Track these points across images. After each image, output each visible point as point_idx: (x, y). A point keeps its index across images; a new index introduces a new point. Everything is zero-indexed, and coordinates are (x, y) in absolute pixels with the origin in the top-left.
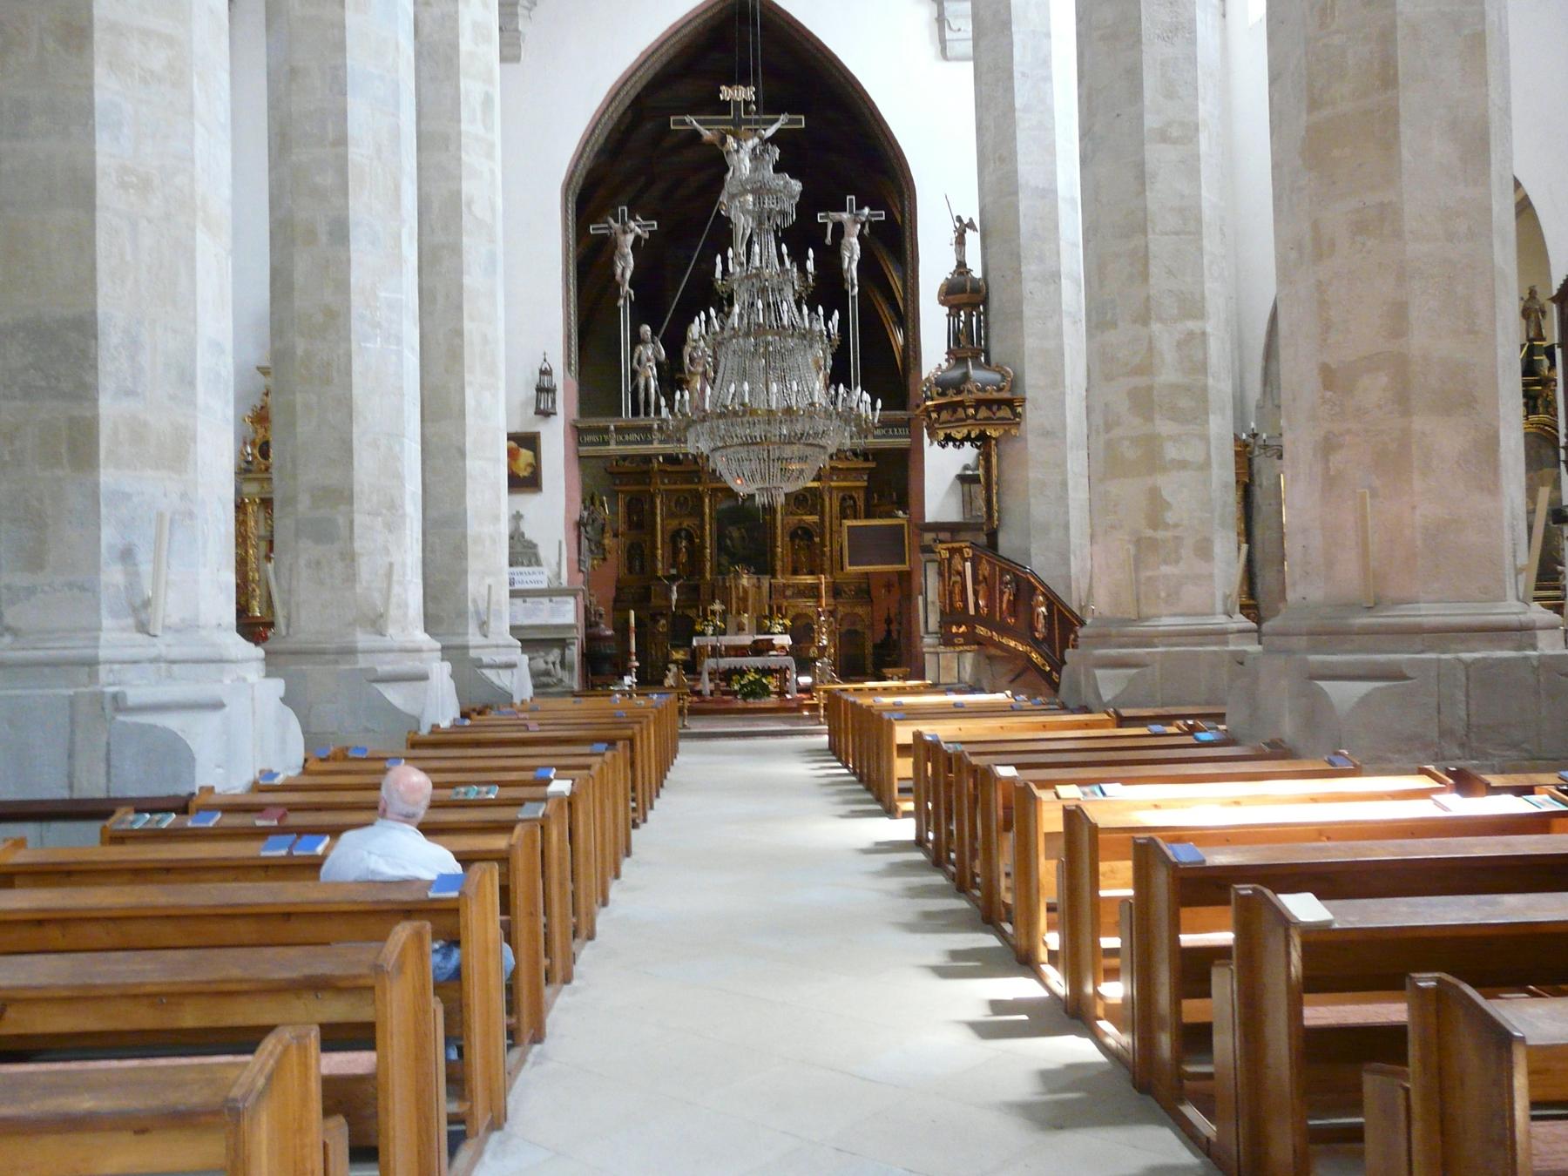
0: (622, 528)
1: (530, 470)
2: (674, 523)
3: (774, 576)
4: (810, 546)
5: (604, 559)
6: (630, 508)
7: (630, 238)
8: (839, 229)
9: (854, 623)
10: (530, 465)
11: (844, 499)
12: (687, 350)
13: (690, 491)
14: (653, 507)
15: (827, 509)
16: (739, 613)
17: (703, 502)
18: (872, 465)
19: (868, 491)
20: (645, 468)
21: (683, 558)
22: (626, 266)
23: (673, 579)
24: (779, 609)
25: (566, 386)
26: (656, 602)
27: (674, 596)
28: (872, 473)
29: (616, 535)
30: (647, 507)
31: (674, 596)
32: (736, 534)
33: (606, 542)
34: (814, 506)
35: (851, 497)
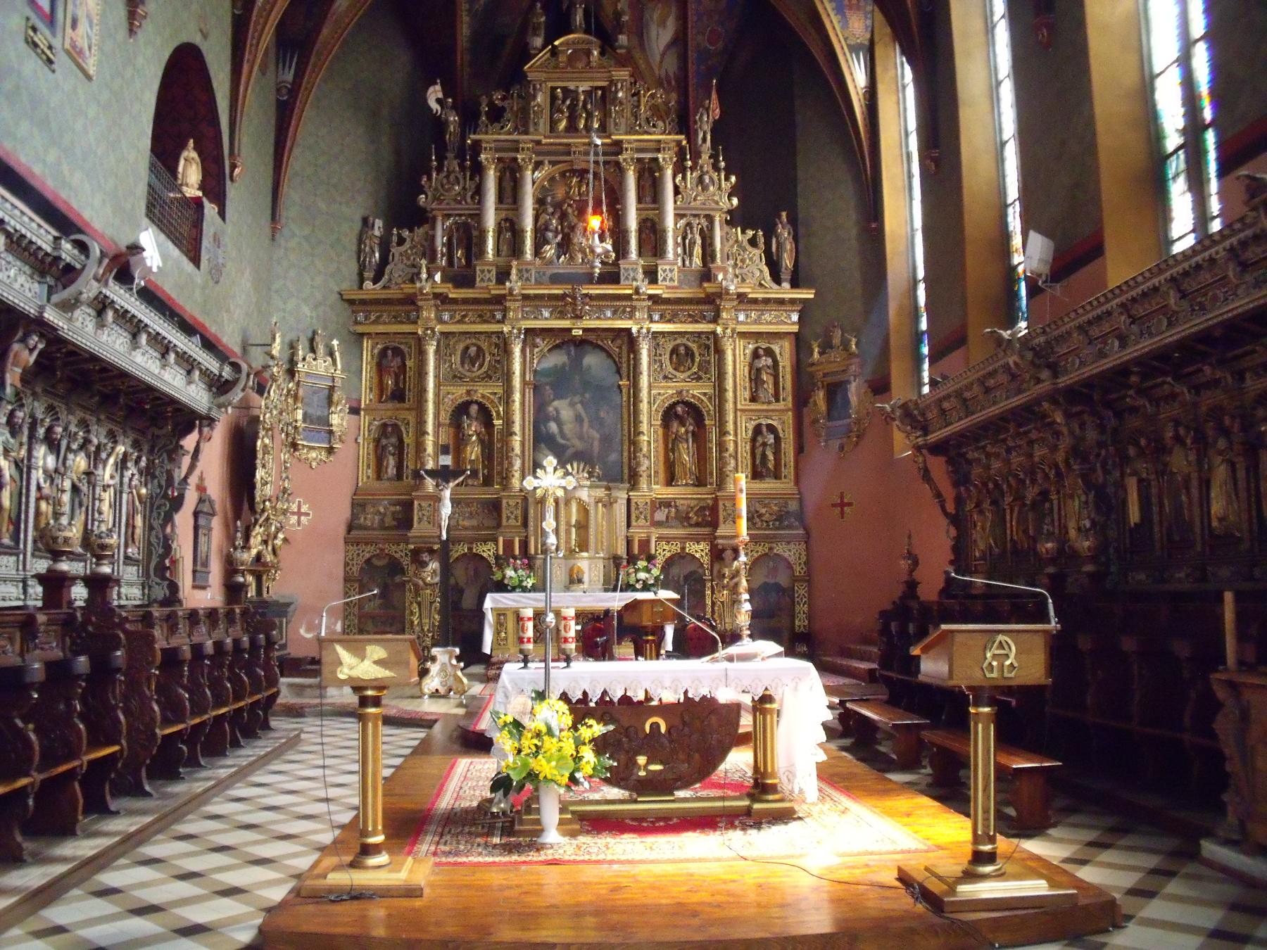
0: (366, 398)
2: (458, 393)
3: (634, 485)
4: (699, 436)
5: (330, 450)
6: (381, 368)
9: (775, 569)
11: (756, 355)
13: (489, 334)
14: (422, 353)
15: (730, 369)
16: (571, 553)
17: (507, 352)
18: (808, 294)
19: (800, 341)
20: (408, 289)
21: (473, 452)
23: (443, 475)
24: (645, 544)
26: (419, 528)
27: (446, 510)
28: (805, 308)
29: (355, 411)
30: (409, 363)
31: (446, 510)
32: (566, 414)
33: (335, 420)
34: (704, 367)
35: (769, 352)
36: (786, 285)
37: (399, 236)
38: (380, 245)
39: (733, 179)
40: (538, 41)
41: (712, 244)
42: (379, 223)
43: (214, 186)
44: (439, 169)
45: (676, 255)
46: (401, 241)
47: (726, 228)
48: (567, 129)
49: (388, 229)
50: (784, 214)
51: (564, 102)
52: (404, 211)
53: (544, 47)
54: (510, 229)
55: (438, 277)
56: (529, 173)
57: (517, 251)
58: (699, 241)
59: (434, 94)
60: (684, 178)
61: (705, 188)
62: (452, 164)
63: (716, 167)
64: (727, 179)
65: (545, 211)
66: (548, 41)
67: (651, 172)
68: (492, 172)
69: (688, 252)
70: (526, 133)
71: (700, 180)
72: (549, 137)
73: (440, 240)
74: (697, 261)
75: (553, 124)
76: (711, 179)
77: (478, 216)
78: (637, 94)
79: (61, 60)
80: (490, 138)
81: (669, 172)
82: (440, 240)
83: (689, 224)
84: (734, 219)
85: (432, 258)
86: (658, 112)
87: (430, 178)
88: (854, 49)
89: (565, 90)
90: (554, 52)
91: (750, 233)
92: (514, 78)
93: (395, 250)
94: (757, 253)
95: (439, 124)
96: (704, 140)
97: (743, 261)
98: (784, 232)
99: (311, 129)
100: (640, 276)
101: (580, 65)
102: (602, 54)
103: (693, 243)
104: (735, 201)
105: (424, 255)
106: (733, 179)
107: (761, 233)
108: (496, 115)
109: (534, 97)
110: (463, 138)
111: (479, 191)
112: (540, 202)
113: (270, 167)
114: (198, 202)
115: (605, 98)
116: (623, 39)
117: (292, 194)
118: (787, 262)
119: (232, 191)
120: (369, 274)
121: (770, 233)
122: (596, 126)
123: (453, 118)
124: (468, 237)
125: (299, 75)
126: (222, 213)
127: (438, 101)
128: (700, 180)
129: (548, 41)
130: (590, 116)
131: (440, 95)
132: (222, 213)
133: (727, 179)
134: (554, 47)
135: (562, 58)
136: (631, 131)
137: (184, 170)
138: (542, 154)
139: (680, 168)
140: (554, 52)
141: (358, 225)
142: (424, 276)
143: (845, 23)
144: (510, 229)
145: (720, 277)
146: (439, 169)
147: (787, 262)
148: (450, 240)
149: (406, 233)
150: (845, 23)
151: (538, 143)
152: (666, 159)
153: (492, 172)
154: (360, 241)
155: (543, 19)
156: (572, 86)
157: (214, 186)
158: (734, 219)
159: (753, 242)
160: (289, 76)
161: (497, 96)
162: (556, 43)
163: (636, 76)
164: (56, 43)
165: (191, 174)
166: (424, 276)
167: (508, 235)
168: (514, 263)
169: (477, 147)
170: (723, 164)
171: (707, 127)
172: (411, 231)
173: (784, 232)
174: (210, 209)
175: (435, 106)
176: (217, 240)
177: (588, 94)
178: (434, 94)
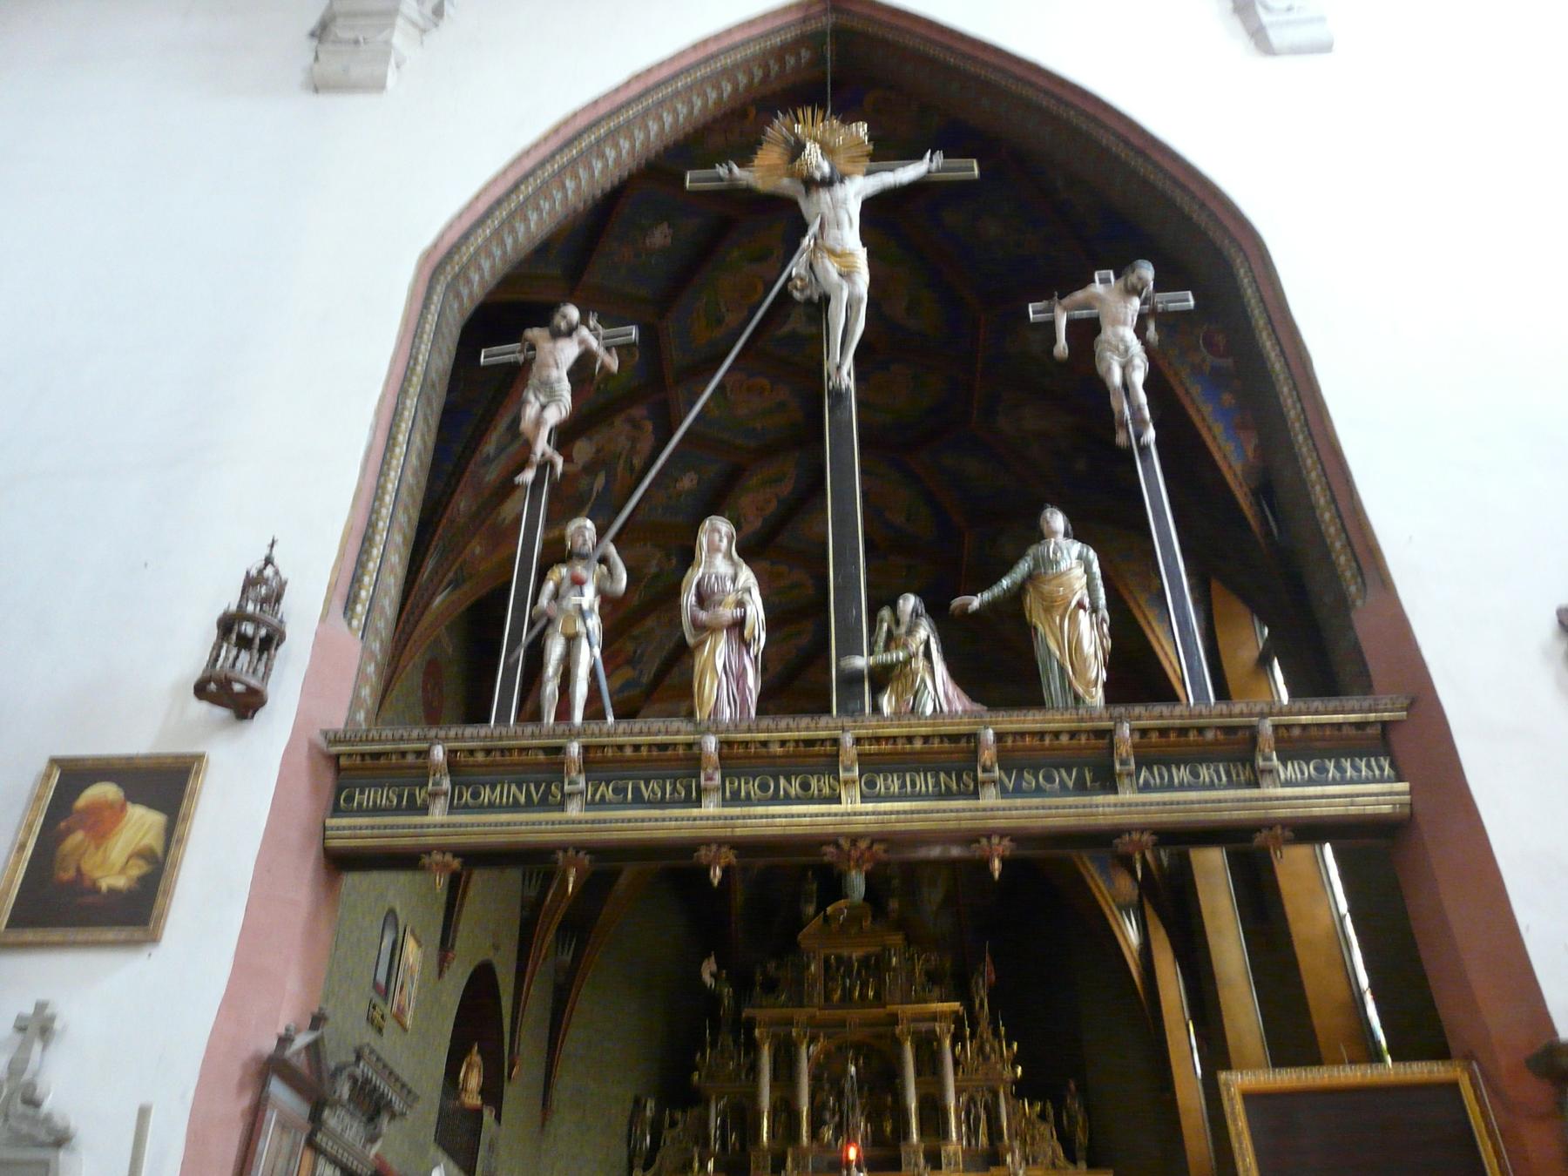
1: (138, 869)
7: (568, 352)
8: (1087, 331)
10: (145, 855)
12: (695, 575)
22: (547, 409)
25: (321, 642)
36: (1083, 1165)
37: (671, 1116)
38: (652, 1127)
39: (1015, 1046)
40: (811, 910)
41: (998, 1118)
42: (650, 1105)
43: (492, 1093)
44: (713, 1045)
45: (960, 1138)
46: (673, 1124)
47: (1012, 1102)
48: (843, 999)
49: (659, 1111)
50: (1072, 1086)
51: (838, 969)
52: (676, 1090)
53: (817, 913)
54: (785, 1110)
55: (710, 1166)
56: (804, 1047)
57: (794, 1136)
58: (983, 1116)
59: (708, 969)
60: (964, 1047)
61: (986, 1058)
62: (727, 1039)
63: (996, 1033)
64: (1009, 1046)
65: (822, 1088)
66: (821, 908)
67: (930, 1042)
68: (766, 1047)
69: (973, 1132)
70: (801, 1005)
71: (981, 1049)
72: (824, 1008)
73: (714, 1122)
74: (983, 1139)
75: (827, 998)
76: (992, 1048)
77: (754, 1097)
78: (911, 958)
79: (390, 1024)
80: (764, 1014)
81: (947, 1043)
82: (714, 1122)
83: (972, 1100)
84: (1022, 1090)
85: (706, 1144)
86: (933, 978)
87: (703, 1055)
88: (1124, 908)
89: (839, 958)
90: (826, 919)
91: (1038, 1108)
92: (787, 945)
93: (668, 1135)
94: (1046, 1129)
95: (714, 998)
96: (982, 1005)
97: (1033, 1138)
98: (1074, 1105)
99: (587, 1005)
100: (922, 1161)
101: (854, 931)
102: (874, 918)
103: (977, 1118)
104: (1019, 1070)
105: (697, 1143)
106: (1015, 1046)
107: (1049, 1105)
108: (771, 987)
109: (808, 967)
110: (738, 1011)
111: (754, 1069)
112: (816, 1079)
113: (545, 1044)
114: (477, 1114)
115: (875, 966)
116: (894, 904)
117: (565, 1081)
118: (1081, 1137)
119: (511, 1092)
120: (639, 1162)
121: (1059, 1106)
122: (871, 994)
123: (727, 991)
124: (743, 1118)
125: (577, 958)
126: (498, 1118)
127: (712, 975)
128: (981, 1049)
129: (821, 908)
130: (864, 986)
131: (714, 968)
132: (498, 1118)
133: (1009, 1046)
134: (826, 916)
135: (834, 926)
136: (906, 1000)
137: (466, 1073)
138: (815, 1029)
139: (957, 1038)
140: (826, 919)
141: (629, 1105)
142: (696, 1165)
143: (1110, 881)
144: (785, 1110)
145: (1009, 1159)
146: (713, 1045)
147: (1081, 1137)
148: (723, 1122)
149: (679, 1115)
150: (1110, 881)
151: (813, 1017)
152: (944, 1029)
153: (766, 1047)
154: (631, 1123)
155: (815, 887)
156: (845, 953)
157: (492, 1093)
158: (1022, 1090)
159: (1042, 1116)
160: (568, 958)
161: (771, 966)
162: (829, 909)
163: (909, 941)
164: (387, 1011)
165: (474, 1081)
166: (696, 1165)
167: (784, 1116)
168: (790, 1151)
169: (750, 1025)
170: (1003, 1029)
171: (983, 993)
172: (684, 1111)
173: (1074, 1105)
174: (488, 1116)
175: (708, 979)
176: (492, 1147)
177: (864, 961)
178: (708, 969)
